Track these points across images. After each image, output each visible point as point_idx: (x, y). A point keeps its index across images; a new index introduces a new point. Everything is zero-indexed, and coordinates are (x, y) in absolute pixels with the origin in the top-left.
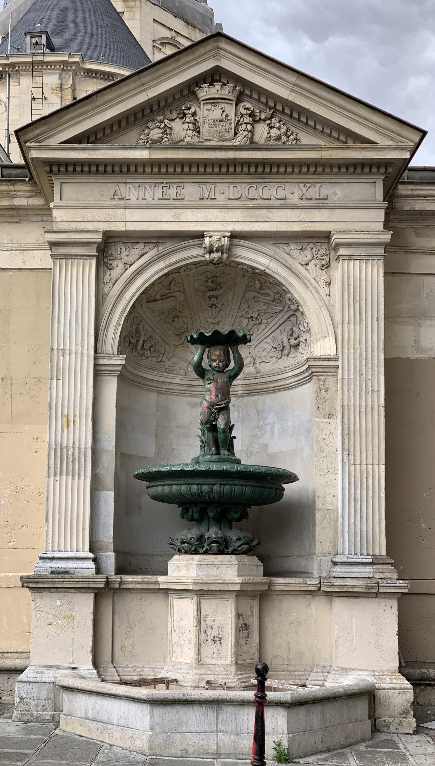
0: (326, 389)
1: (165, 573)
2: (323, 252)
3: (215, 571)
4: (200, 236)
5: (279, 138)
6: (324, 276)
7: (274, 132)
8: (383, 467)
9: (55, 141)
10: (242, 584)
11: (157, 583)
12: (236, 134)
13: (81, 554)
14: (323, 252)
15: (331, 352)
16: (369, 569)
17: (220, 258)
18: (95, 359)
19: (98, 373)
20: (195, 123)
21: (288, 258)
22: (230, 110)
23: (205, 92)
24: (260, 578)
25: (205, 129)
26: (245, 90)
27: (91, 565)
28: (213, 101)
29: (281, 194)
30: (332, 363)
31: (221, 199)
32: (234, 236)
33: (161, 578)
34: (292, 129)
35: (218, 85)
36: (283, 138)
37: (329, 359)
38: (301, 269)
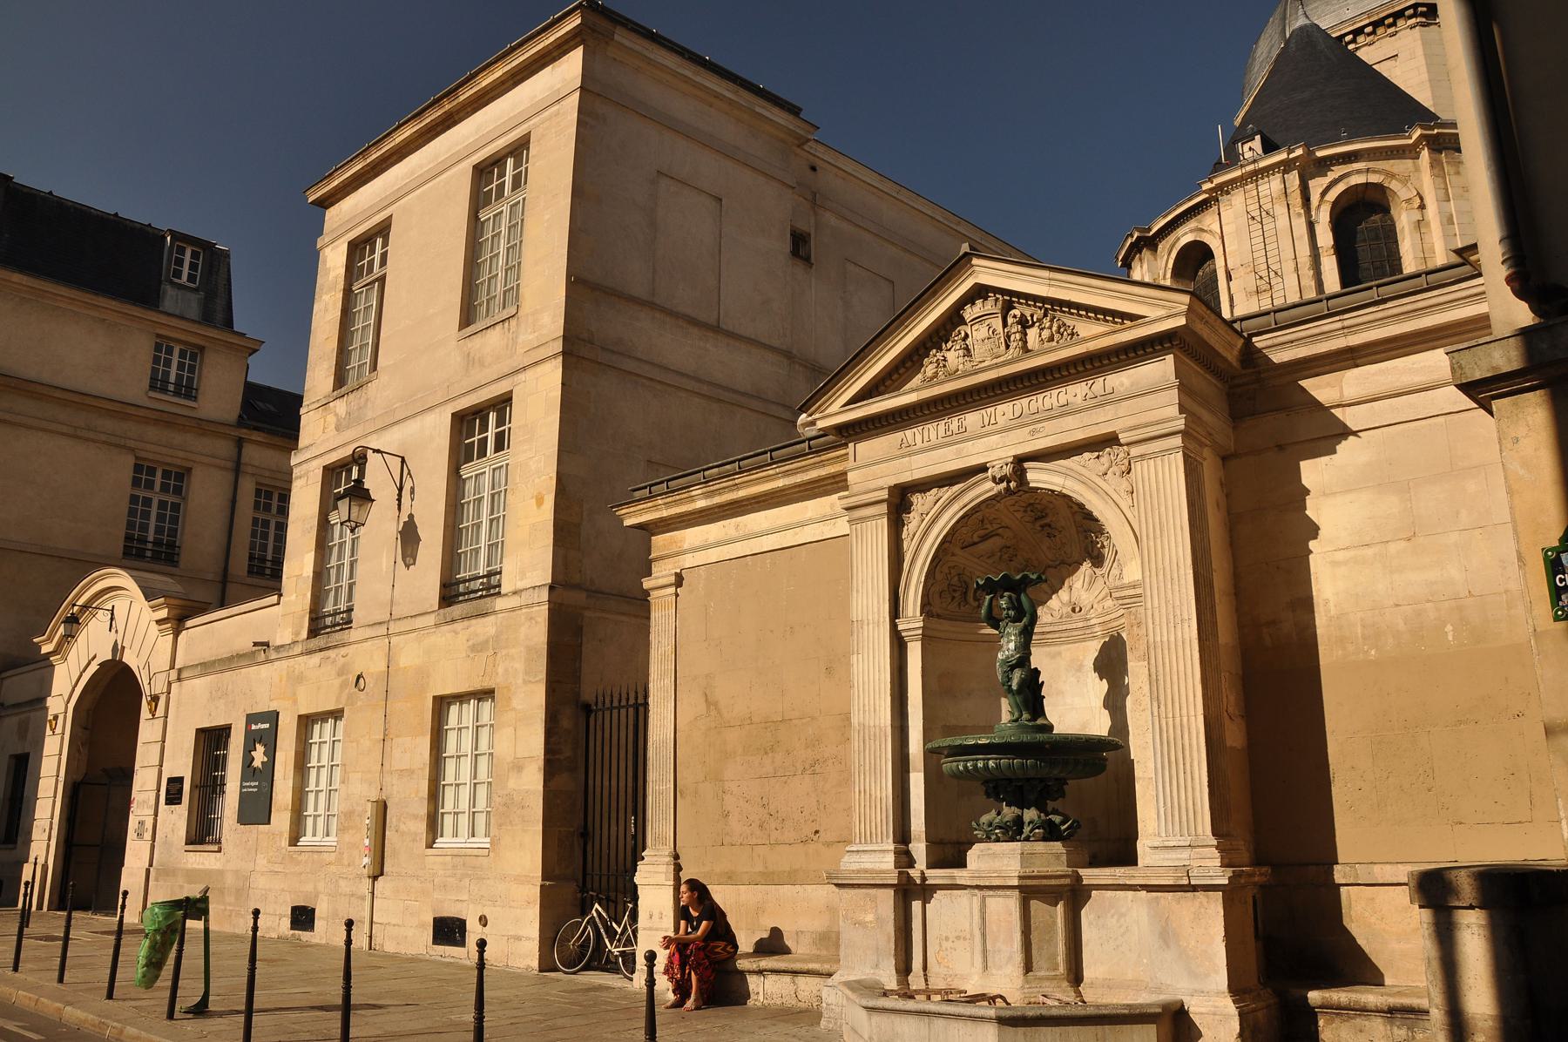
0: (1139, 625)
1: (962, 864)
2: (1122, 455)
3: (997, 864)
4: (983, 468)
5: (1051, 339)
6: (1124, 485)
7: (1046, 334)
8: (1201, 719)
9: (835, 407)
10: (1020, 878)
11: (953, 877)
12: (1008, 347)
13: (886, 847)
14: (1122, 455)
15: (1137, 576)
16: (1185, 854)
17: (1008, 489)
18: (894, 626)
19: (899, 645)
20: (967, 349)
21: (1083, 471)
22: (997, 323)
23: (969, 313)
24: (1062, 868)
25: (979, 352)
26: (1010, 298)
27: (891, 858)
28: (979, 319)
29: (1063, 401)
30: (1139, 591)
31: (1002, 421)
32: (1020, 461)
33: (956, 872)
34: (1068, 322)
35: (979, 302)
36: (1056, 337)
37: (1134, 587)
38: (1099, 481)
